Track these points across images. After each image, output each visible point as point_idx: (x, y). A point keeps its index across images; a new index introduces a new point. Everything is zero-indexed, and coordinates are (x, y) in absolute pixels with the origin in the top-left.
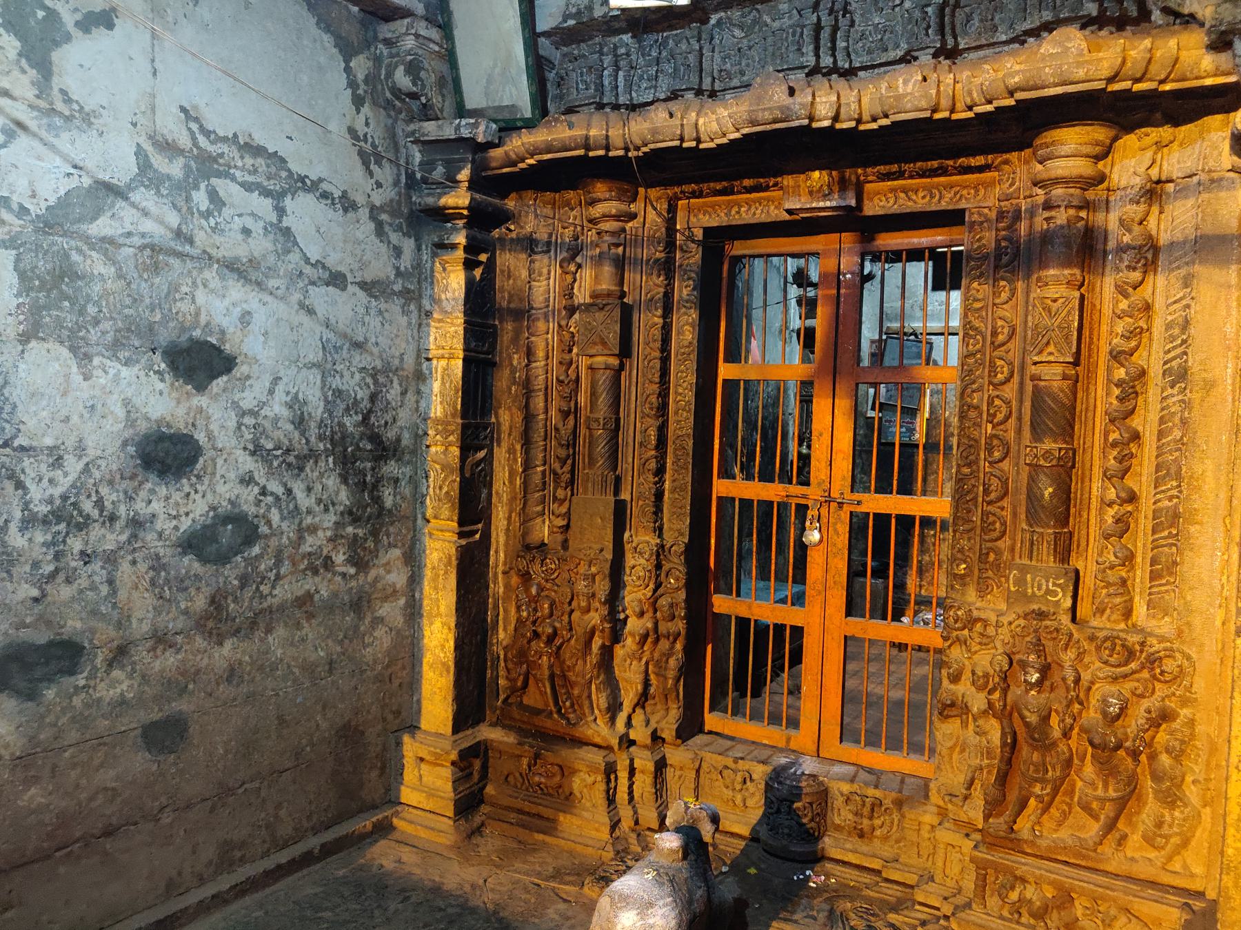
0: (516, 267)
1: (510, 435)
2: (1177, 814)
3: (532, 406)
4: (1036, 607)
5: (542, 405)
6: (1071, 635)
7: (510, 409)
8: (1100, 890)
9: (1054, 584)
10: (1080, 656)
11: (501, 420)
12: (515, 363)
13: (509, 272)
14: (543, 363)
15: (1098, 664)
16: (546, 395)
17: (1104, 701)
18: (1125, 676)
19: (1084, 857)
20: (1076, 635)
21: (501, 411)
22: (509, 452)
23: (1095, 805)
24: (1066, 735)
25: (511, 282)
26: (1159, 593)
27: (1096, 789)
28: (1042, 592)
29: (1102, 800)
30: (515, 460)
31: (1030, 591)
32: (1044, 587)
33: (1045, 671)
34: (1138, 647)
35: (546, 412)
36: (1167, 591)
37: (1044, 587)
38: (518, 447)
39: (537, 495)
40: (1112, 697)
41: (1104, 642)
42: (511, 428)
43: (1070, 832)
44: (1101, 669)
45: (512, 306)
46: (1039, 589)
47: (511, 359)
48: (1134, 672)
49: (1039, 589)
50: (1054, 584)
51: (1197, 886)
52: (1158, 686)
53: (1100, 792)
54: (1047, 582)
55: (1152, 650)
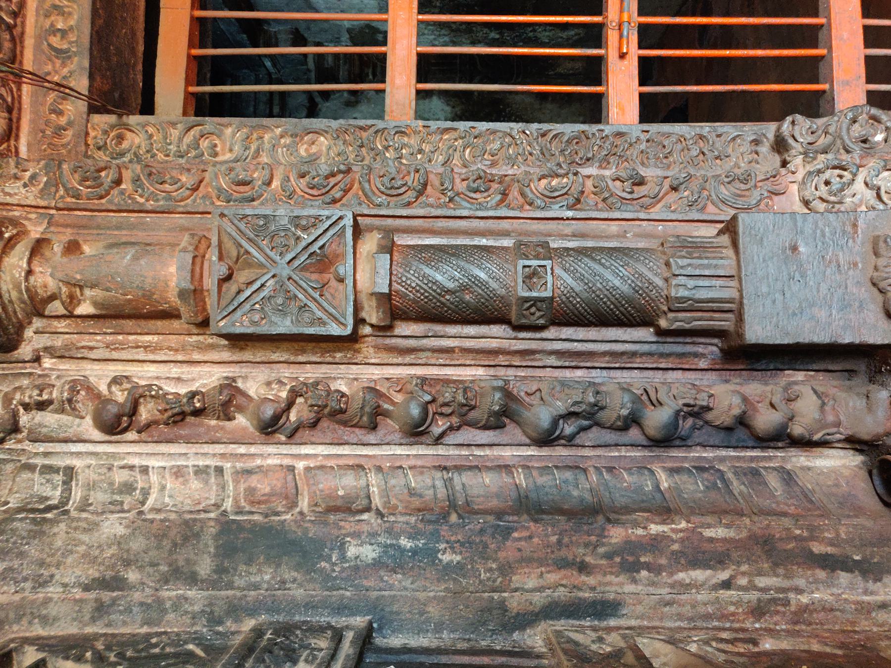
0: (89, 559)
1: (583, 568)
3: (494, 503)
5: (488, 478)
7: (506, 569)
11: (539, 600)
12: (369, 553)
13: (103, 584)
14: (374, 479)
16: (458, 468)
21: (515, 603)
22: (631, 568)
25: (132, 576)
30: (656, 543)
35: (506, 468)
38: (617, 535)
39: (737, 486)
42: (563, 564)
45: (205, 567)
47: (358, 569)
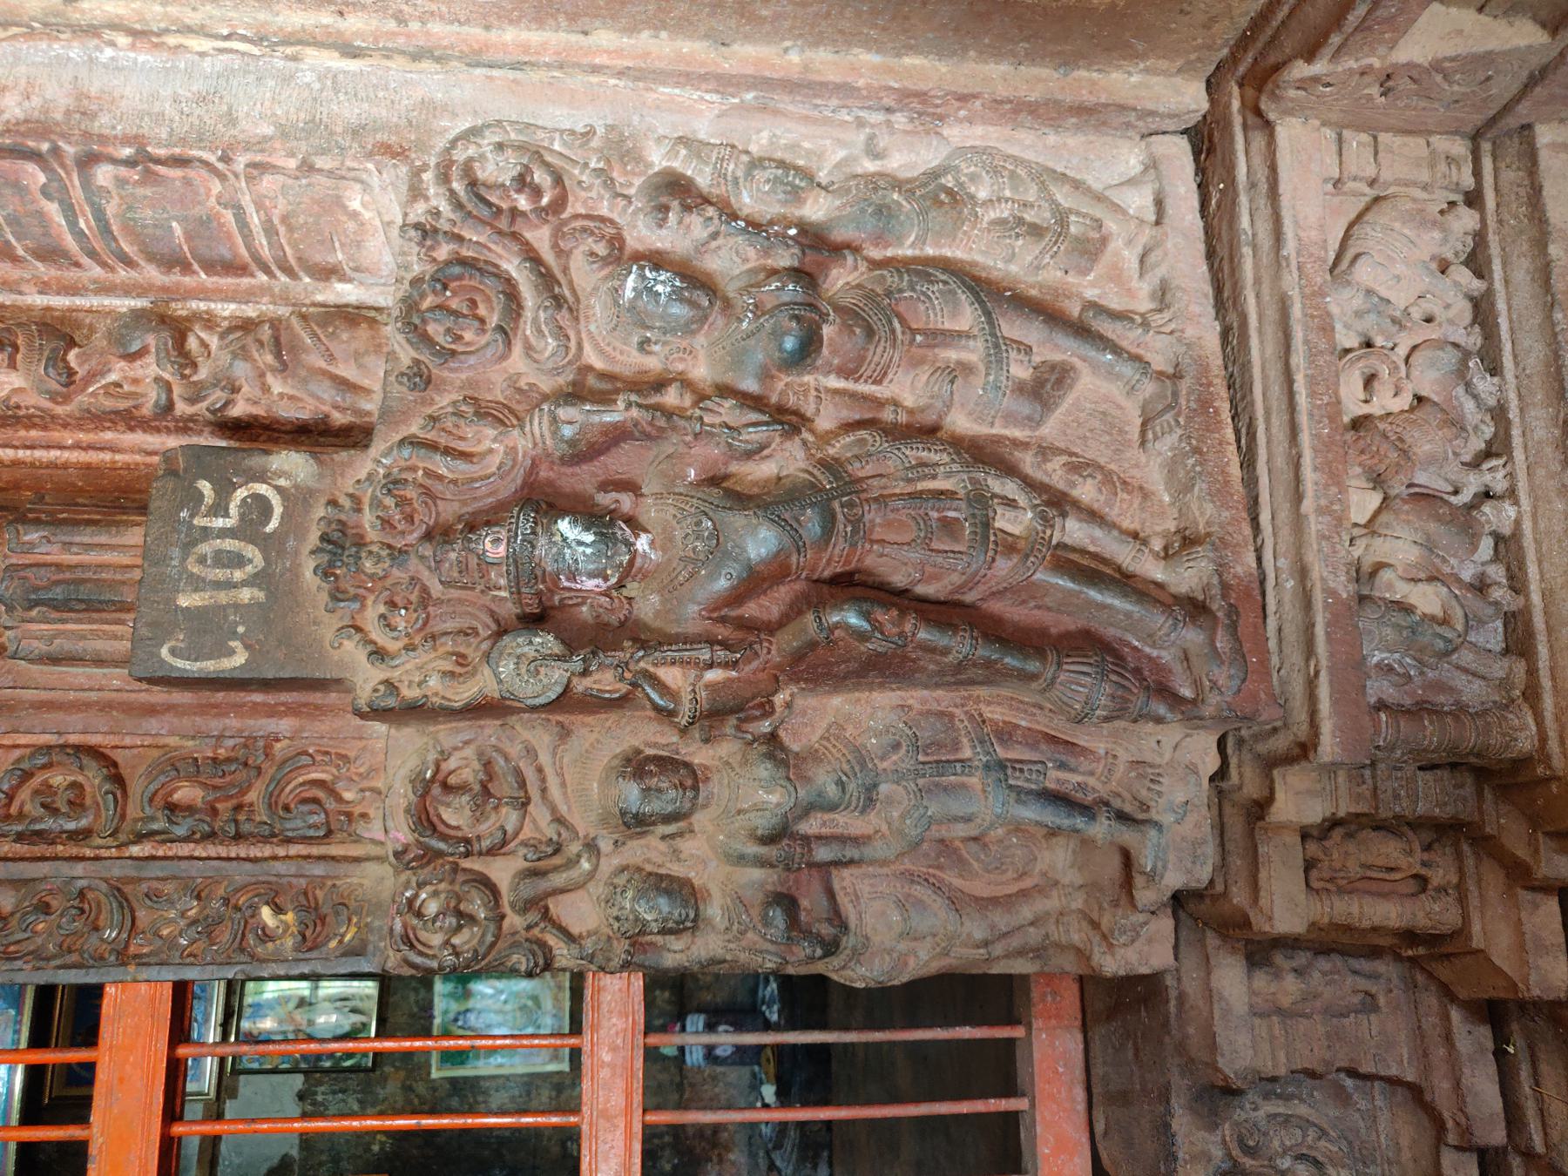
2: (982, 194)
4: (308, 566)
6: (412, 442)
8: (1298, 335)
9: (220, 509)
10: (484, 412)
15: (517, 361)
17: (636, 316)
18: (546, 280)
19: (1205, 403)
20: (414, 428)
23: (1020, 371)
24: (789, 420)
26: (270, 230)
27: (966, 369)
28: (251, 551)
29: (998, 347)
31: (246, 595)
32: (229, 544)
33: (542, 501)
34: (444, 252)
36: (259, 206)
37: (229, 544)
40: (616, 292)
41: (426, 340)
43: (1134, 453)
44: (528, 348)
46: (239, 561)
48: (532, 258)
49: (239, 561)
50: (220, 509)
51: (1178, 152)
52: (575, 207)
53: (973, 353)
54: (206, 533)
55: (444, 207)
